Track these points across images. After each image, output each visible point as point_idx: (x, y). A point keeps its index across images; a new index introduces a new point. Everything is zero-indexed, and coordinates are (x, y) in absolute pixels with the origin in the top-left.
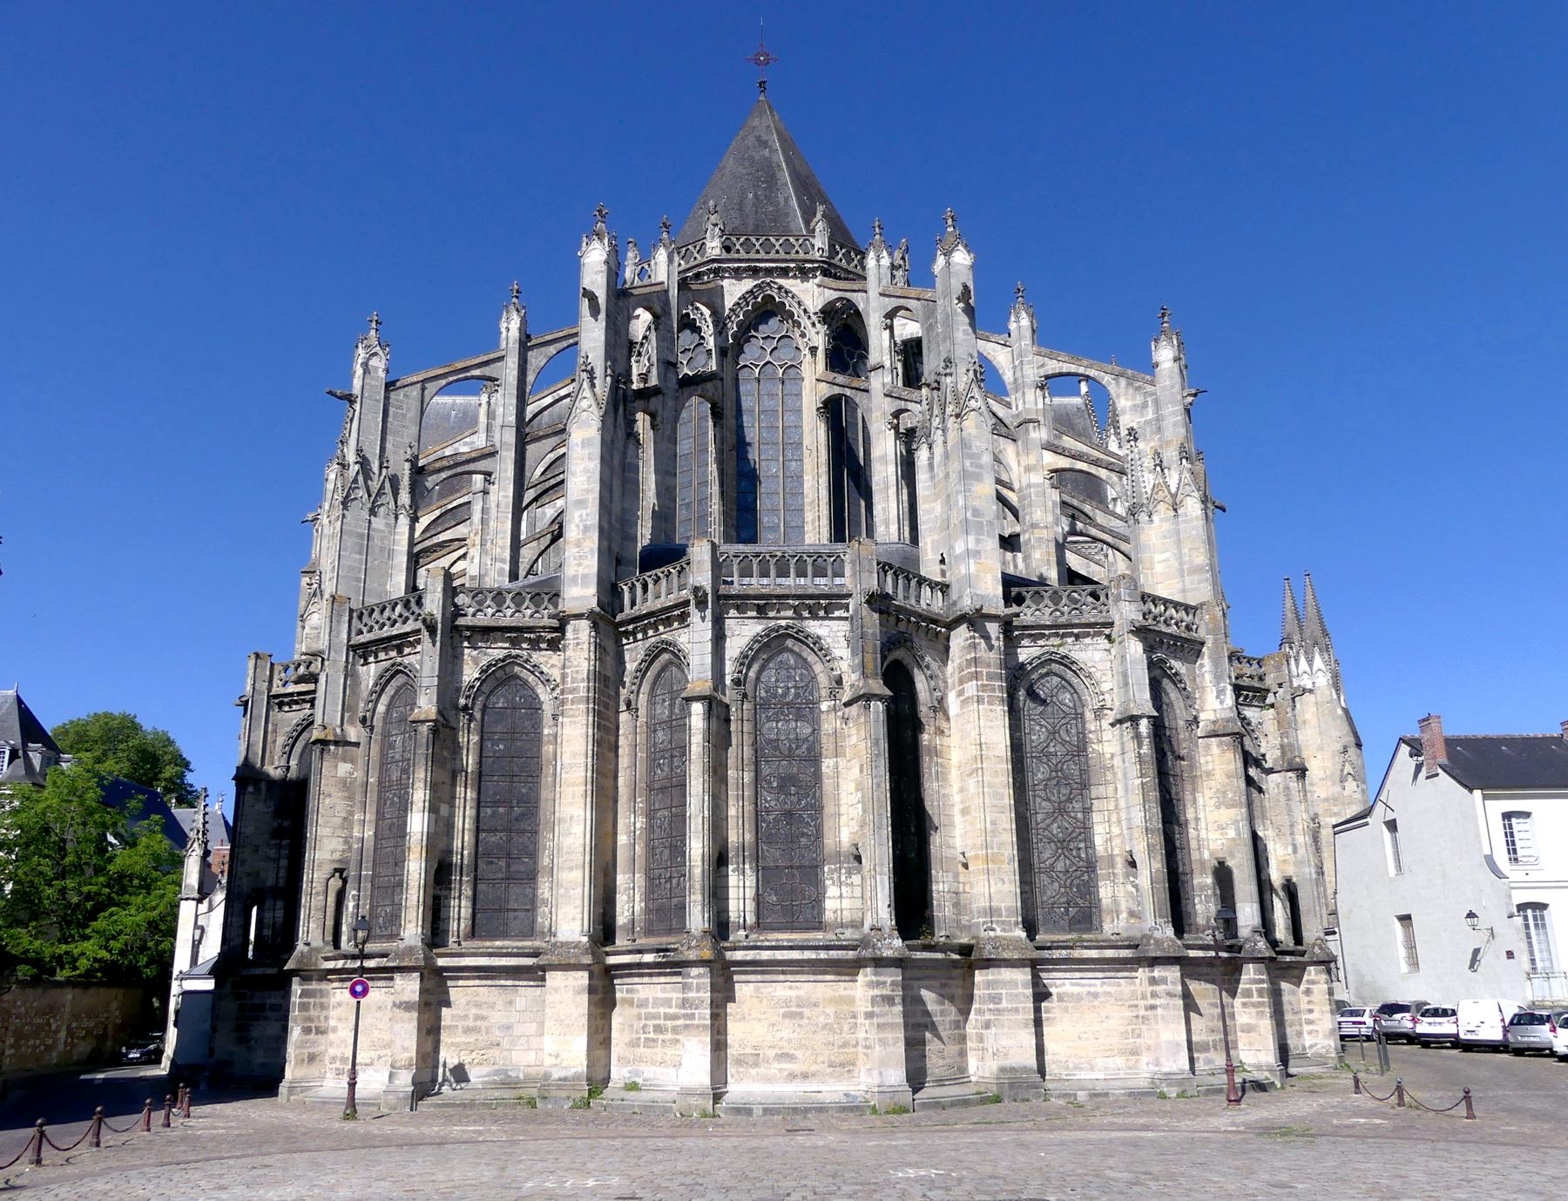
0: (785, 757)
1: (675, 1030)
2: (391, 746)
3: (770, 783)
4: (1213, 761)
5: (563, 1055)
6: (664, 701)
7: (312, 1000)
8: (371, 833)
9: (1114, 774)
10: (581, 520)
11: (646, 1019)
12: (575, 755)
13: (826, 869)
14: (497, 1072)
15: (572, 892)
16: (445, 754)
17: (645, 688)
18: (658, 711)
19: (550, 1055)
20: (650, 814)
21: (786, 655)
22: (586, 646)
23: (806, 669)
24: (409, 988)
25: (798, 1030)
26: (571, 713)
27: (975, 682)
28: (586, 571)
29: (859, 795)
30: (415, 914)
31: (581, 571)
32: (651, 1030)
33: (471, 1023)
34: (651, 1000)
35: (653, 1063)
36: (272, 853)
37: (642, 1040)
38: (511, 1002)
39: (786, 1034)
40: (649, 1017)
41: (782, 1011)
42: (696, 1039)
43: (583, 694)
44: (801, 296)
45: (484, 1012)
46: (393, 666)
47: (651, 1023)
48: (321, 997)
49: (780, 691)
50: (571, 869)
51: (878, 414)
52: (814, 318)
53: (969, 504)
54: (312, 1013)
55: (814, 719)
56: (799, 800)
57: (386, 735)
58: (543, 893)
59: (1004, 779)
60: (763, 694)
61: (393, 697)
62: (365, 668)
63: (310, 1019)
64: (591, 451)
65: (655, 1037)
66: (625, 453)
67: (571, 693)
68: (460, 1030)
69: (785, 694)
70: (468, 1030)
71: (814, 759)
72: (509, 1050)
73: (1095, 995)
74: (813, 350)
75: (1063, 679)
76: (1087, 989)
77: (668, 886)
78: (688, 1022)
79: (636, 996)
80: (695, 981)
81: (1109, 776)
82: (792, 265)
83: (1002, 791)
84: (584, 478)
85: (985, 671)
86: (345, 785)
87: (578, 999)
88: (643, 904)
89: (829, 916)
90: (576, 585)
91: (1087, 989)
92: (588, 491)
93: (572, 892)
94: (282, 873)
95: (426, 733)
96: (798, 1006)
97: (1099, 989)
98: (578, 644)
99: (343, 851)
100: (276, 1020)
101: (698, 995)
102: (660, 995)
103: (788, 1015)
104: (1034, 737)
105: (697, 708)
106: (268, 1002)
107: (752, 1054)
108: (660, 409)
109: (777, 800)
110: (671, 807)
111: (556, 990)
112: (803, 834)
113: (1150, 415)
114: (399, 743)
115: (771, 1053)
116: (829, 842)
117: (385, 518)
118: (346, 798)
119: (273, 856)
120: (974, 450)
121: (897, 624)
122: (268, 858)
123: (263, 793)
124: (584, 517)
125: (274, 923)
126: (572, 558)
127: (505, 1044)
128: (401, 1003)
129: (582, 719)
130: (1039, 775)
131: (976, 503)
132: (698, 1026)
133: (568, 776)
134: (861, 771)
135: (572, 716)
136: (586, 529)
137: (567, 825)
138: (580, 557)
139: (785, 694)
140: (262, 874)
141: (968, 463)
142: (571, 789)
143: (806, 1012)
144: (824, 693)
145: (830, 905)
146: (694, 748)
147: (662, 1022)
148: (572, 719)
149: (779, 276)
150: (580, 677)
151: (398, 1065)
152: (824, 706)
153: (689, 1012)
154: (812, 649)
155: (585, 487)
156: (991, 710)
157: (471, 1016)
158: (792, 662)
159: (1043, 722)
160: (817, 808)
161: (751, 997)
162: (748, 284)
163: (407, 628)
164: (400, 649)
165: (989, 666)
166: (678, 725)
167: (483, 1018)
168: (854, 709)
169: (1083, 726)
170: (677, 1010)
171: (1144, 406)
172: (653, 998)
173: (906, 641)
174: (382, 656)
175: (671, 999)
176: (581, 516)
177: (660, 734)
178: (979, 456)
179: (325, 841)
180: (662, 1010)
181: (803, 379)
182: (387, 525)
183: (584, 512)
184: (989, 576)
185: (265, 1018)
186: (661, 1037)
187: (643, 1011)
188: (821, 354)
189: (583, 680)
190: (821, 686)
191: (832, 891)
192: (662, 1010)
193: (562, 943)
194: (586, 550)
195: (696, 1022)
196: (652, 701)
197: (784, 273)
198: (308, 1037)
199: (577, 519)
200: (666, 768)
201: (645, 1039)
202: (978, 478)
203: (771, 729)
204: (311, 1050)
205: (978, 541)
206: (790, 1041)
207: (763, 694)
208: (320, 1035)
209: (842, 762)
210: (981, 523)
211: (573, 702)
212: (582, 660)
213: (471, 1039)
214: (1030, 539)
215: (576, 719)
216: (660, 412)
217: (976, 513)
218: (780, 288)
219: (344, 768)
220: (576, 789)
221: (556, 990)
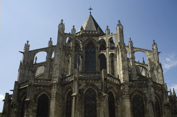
3: (87, 112)
4: (165, 111)
9: (149, 112)
16: (31, 106)
18: (68, 100)
21: (91, 89)
22: (56, 88)
23: (94, 92)
27: (124, 95)
29: (103, 114)
44: (95, 40)
49: (89, 96)
52: (98, 43)
53: (123, 65)
55: (95, 101)
59: (129, 112)
60: (86, 96)
66: (65, 58)
67: (53, 96)
69: (90, 96)
74: (98, 48)
75: (140, 96)
81: (148, 112)
82: (94, 35)
83: (129, 114)
85: (126, 93)
86: (15, 112)
104: (134, 106)
105: (74, 98)
108: (72, 53)
113: (152, 56)
118: (16, 115)
120: (124, 57)
121: (110, 85)
129: (54, 101)
130: (135, 112)
131: (124, 65)
134: (104, 109)
135: (53, 100)
139: (90, 96)
141: (123, 58)
146: (73, 104)
149: (92, 36)
154: (95, 88)
156: (127, 100)
159: (136, 103)
162: (87, 38)
163: (27, 86)
164: (25, 89)
165: (127, 93)
166: (71, 102)
169: (143, 104)
171: (151, 55)
173: (112, 88)
177: (68, 103)
178: (125, 58)
181: (96, 52)
184: (127, 78)
188: (99, 49)
189: (55, 94)
196: (67, 98)
197: (93, 36)
200: (69, 109)
202: (124, 61)
205: (125, 71)
207: (86, 96)
209: (100, 108)
210: (125, 69)
211: (53, 98)
214: (132, 77)
216: (72, 54)
217: (124, 67)
218: (92, 38)
219: (15, 110)
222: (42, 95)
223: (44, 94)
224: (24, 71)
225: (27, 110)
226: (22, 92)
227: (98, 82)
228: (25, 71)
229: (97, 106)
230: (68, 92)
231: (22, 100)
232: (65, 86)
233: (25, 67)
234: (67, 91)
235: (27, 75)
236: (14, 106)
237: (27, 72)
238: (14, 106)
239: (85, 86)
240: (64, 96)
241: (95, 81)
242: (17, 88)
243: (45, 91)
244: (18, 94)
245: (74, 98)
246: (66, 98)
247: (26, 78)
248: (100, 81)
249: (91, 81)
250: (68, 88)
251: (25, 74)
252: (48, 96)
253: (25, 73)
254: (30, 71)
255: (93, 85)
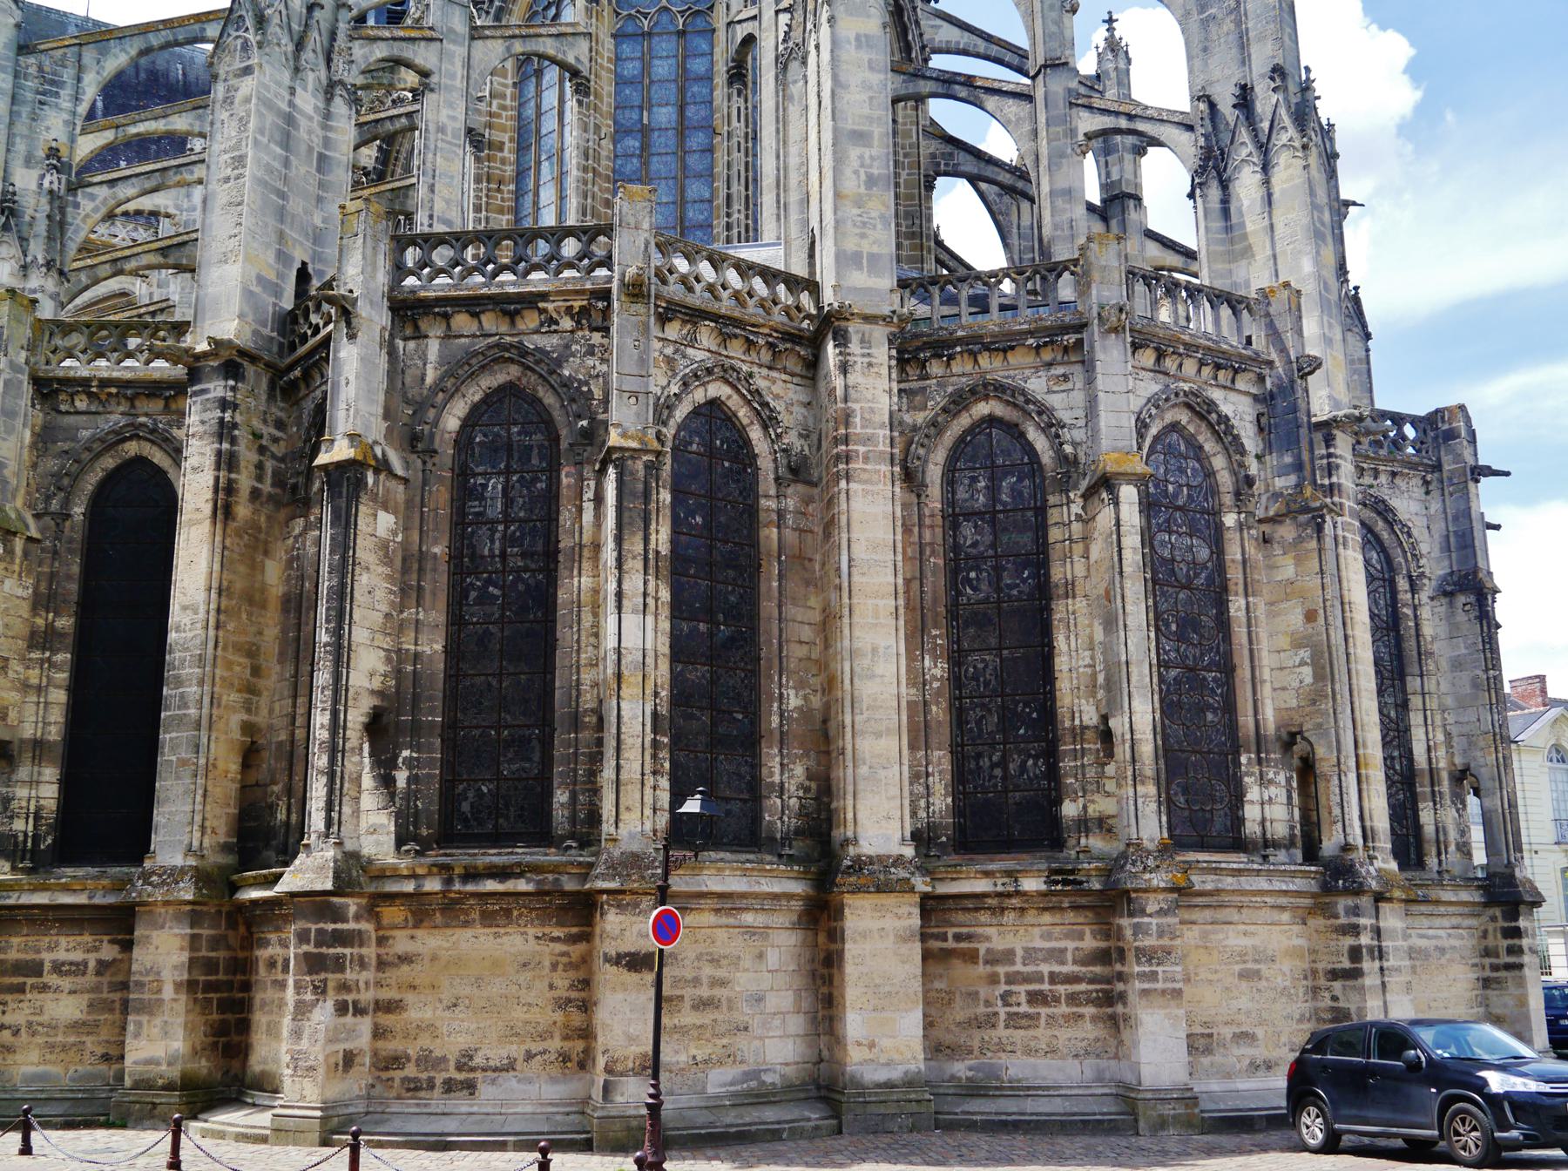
0: (1183, 587)
1: (1073, 999)
2: (479, 494)
5: (885, 1043)
6: (974, 480)
7: (347, 951)
8: (438, 647)
10: (862, 166)
11: (1008, 982)
12: (875, 547)
13: (1243, 759)
14: (748, 1076)
15: (882, 773)
17: (939, 456)
19: (859, 1044)
20: (956, 659)
22: (885, 371)
23: (1199, 460)
24: (635, 928)
25: (1257, 997)
26: (865, 476)
28: (875, 249)
30: (638, 796)
31: (866, 247)
32: (1023, 998)
33: (704, 992)
34: (1020, 953)
35: (1029, 1052)
36: (34, 676)
37: (1002, 1016)
38: (761, 956)
39: (1244, 1003)
40: (1012, 979)
41: (1237, 968)
42: (1162, 1012)
43: (884, 447)
45: (721, 973)
46: (490, 347)
47: (1022, 989)
48: (361, 946)
49: (1171, 488)
50: (878, 735)
51: (1059, 129)
54: (350, 975)
56: (1202, 655)
57: (462, 473)
58: (771, 774)
61: (475, 408)
62: (412, 345)
63: (344, 987)
64: (873, 56)
65: (1032, 1011)
68: (687, 1003)
69: (1176, 495)
70: (702, 1004)
71: (1219, 594)
72: (761, 1038)
73: (1442, 950)
76: (1434, 942)
77: (998, 772)
78: (1146, 986)
79: (982, 948)
80: (1154, 921)
84: (864, 97)
87: (904, 949)
88: (949, 800)
89: (1252, 828)
90: (860, 268)
91: (1434, 942)
92: (870, 119)
93: (882, 773)
94: (57, 716)
95: (641, 473)
96: (1256, 961)
97: (1446, 943)
98: (870, 365)
99: (385, 676)
100: (72, 992)
101: (1161, 942)
102: (1039, 943)
103: (1245, 975)
105: (1129, 493)
106: (47, 957)
107: (1202, 1035)
109: (1178, 651)
110: (1000, 649)
111: (864, 935)
112: (1209, 707)
114: (495, 485)
115: (1227, 1032)
116: (1246, 721)
117: (314, 96)
119: (34, 681)
122: (25, 687)
123: (18, 561)
124: (868, 161)
125: (39, 809)
126: (849, 223)
127: (755, 1023)
128: (619, 956)
132: (1164, 992)
133: (864, 579)
135: (866, 482)
136: (871, 181)
137: (866, 662)
138: (864, 224)
140: (13, 715)
142: (870, 602)
143: (1262, 966)
144: (1228, 499)
145: (1251, 813)
147: (1046, 987)
148: (869, 487)
150: (877, 418)
151: (619, 1067)
152: (1230, 520)
153: (1147, 969)
155: (867, 111)
157: (705, 980)
158: (1183, 448)
160: (1227, 668)
161: (1197, 947)
164: (512, 316)
167: (723, 983)
168: (1287, 531)
170: (1076, 968)
172: (1026, 950)
174: (462, 322)
175: (1063, 951)
176: (861, 157)
179: (361, 650)
180: (1045, 968)
182: (316, 108)
183: (867, 153)
185: (44, 988)
186: (1044, 1011)
187: (1002, 970)
189: (882, 426)
190: (1222, 489)
191: (1253, 793)
192: (1045, 968)
193: (871, 859)
194: (874, 214)
195: (1160, 985)
198: (342, 1020)
199: (855, 164)
200: (984, 587)
201: (1008, 1014)
203: (1163, 543)
204: (348, 1046)
206: (1248, 1013)
208: (359, 1019)
211: (866, 459)
212: (879, 392)
213: (706, 1018)
215: (875, 488)
220: (881, 603)
221: (864, 935)
222: (696, 412)
223: (714, 403)
224: (286, 76)
225: (639, 548)
226: (448, 336)
227: (1230, 388)
228: (299, 90)
229: (1231, 587)
230: (964, 421)
231: (452, 422)
232: (935, 368)
233: (299, 46)
234: (956, 415)
235: (310, 132)
236: (370, 480)
237: (308, 101)
238: (376, 482)
239: (1153, 401)
240: (921, 451)
241: (1218, 367)
242: (382, 278)
243: (727, 373)
244: (392, 353)
245: (1129, 493)
246: (934, 473)
247: (303, 170)
248: (1251, 375)
249: (1190, 367)
250: (973, 391)
251: (290, 120)
252: (755, 434)
253: (291, 104)
254: (338, 101)
255: (1203, 410)
